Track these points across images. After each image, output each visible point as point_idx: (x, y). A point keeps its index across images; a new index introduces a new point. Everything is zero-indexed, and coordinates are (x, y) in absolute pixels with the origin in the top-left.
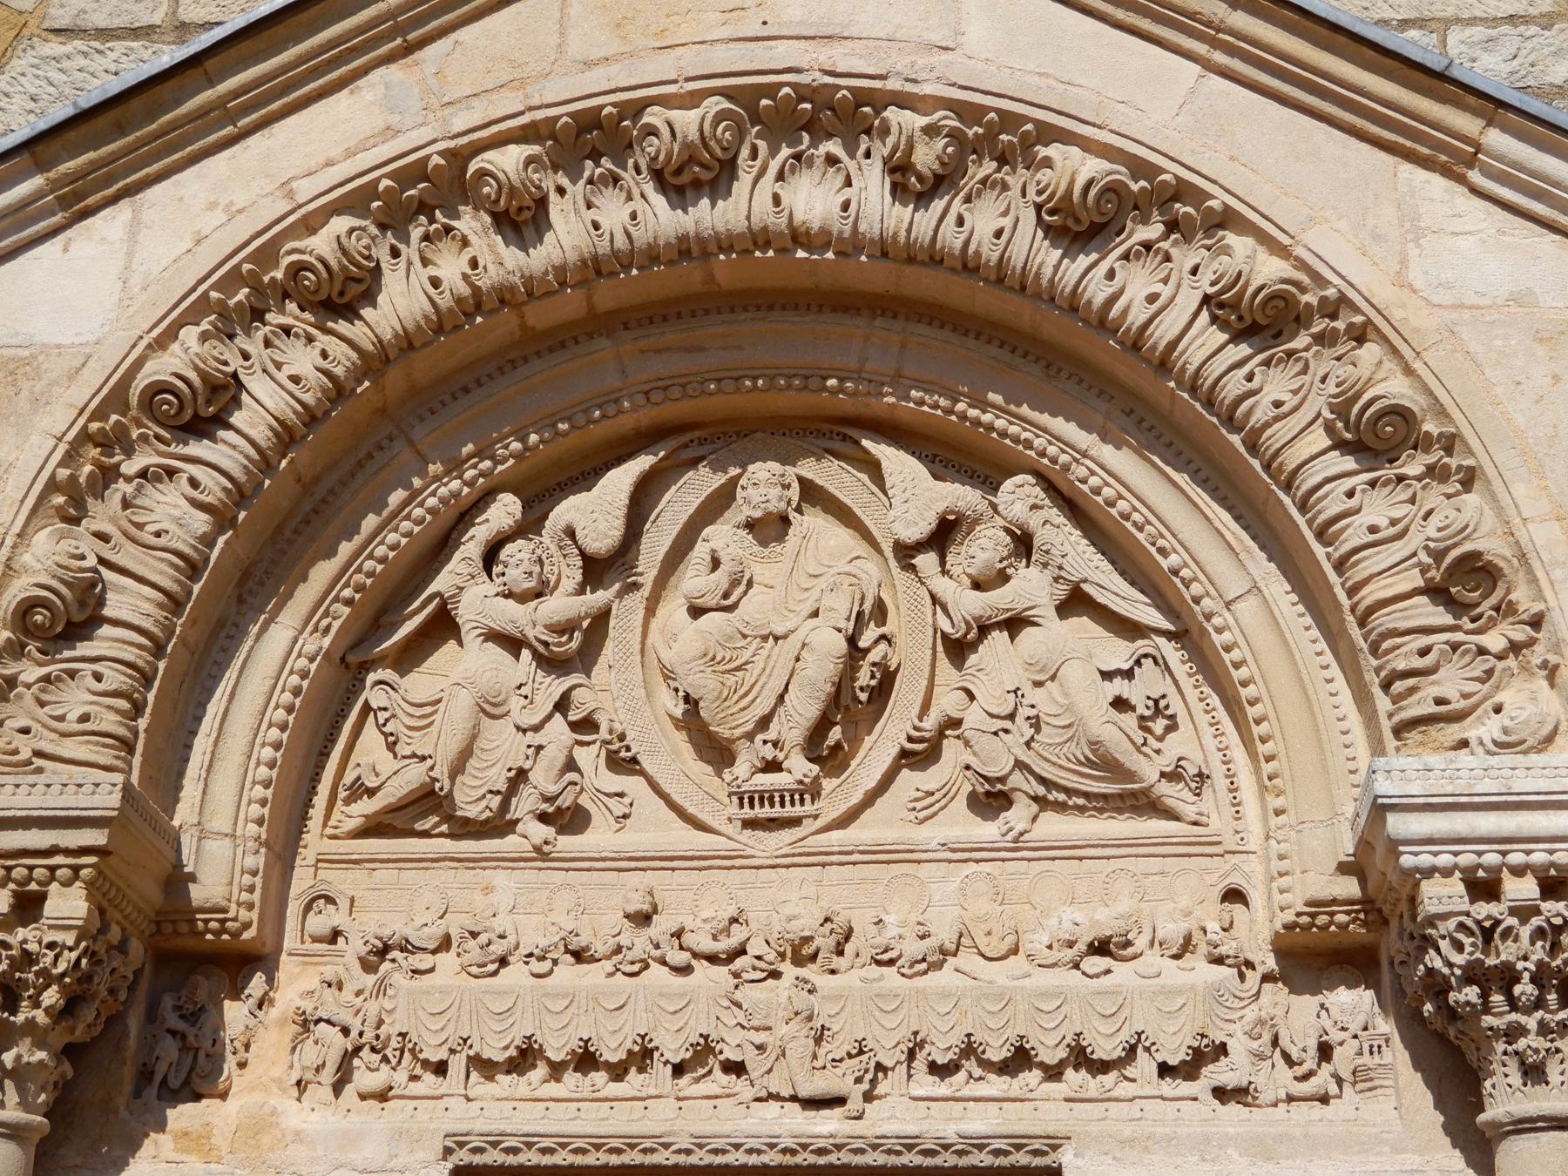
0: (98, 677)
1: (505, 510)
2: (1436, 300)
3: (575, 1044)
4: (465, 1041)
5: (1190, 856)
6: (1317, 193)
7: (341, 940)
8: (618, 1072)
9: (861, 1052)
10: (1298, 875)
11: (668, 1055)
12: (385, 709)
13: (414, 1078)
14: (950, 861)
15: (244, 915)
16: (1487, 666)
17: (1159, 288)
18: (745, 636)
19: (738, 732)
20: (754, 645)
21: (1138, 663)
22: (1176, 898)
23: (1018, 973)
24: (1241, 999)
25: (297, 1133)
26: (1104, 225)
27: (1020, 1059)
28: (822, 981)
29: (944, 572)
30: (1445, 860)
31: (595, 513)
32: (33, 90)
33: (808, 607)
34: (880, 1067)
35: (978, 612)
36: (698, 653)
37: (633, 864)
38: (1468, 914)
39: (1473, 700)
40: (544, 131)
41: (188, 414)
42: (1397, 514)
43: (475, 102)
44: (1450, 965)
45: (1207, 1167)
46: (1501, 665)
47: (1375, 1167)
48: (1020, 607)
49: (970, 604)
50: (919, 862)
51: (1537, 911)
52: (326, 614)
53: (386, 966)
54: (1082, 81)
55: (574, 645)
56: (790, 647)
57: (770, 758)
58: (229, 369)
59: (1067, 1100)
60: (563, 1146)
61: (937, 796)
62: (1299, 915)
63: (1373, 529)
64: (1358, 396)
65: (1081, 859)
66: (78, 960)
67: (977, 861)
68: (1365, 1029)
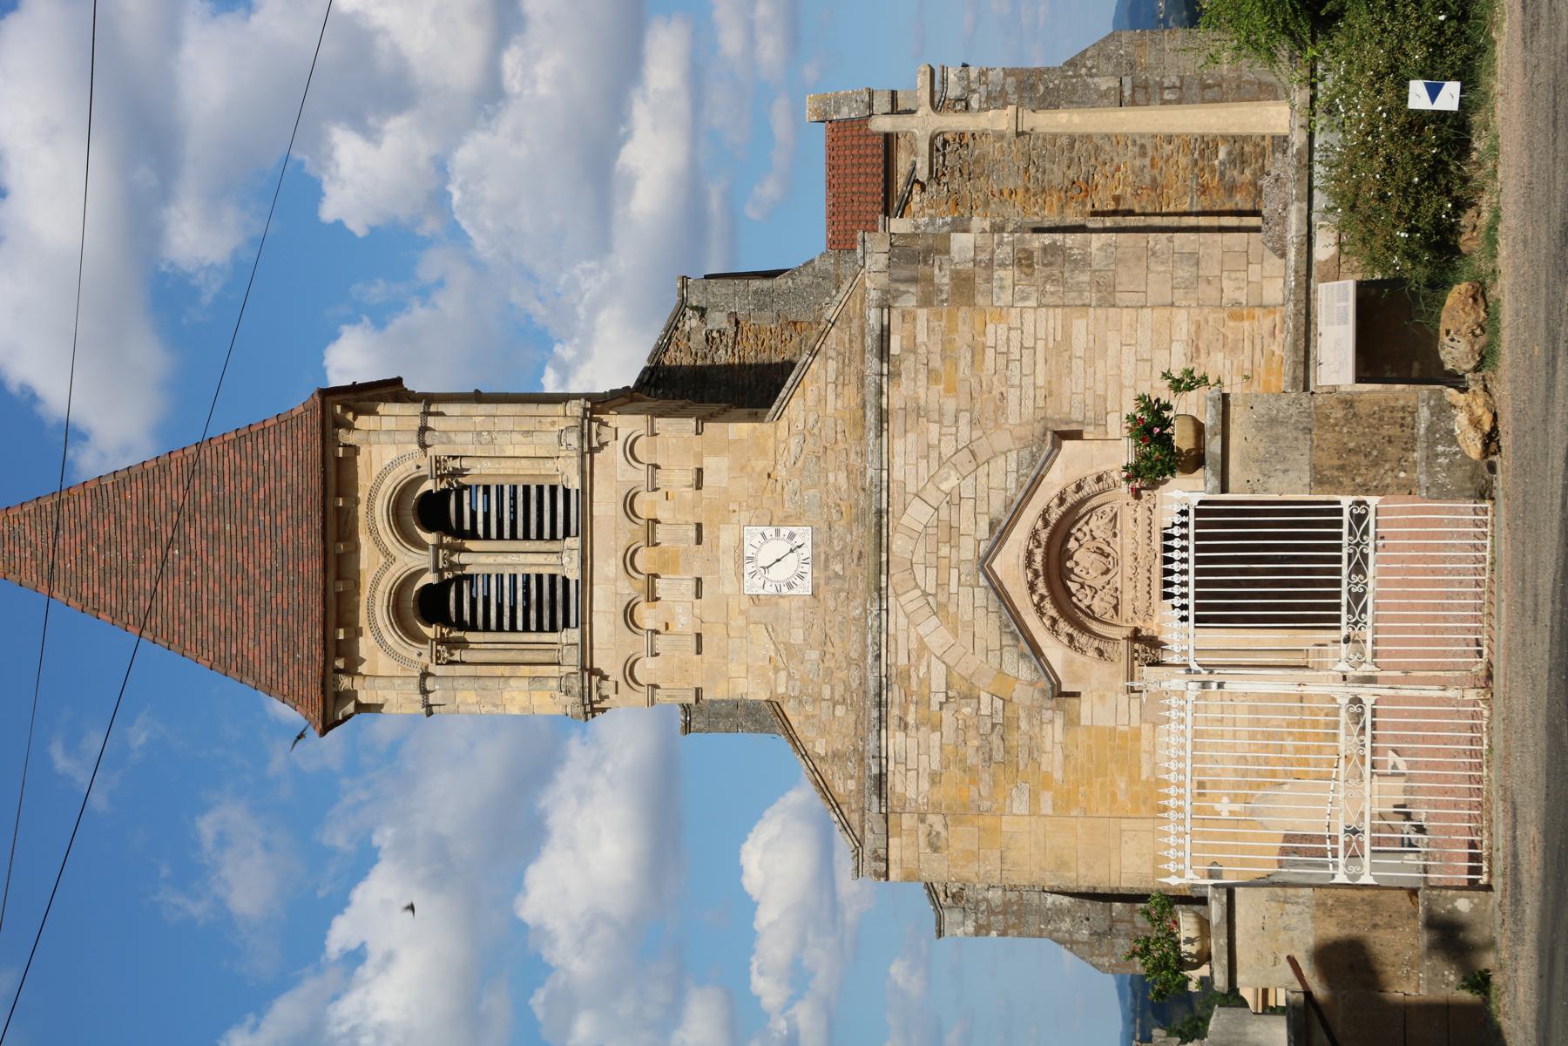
6: (1046, 494)
22: (1128, 511)
31: (1073, 587)
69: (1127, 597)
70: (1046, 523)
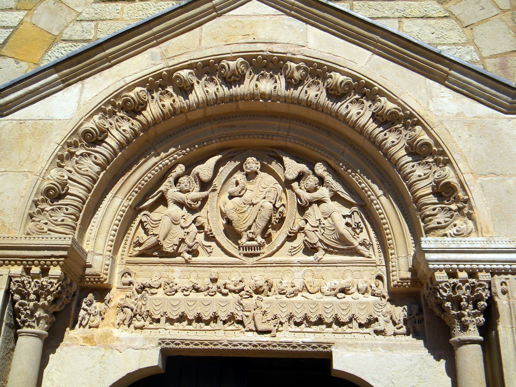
0: (67, 210)
1: (180, 169)
2: (437, 114)
3: (196, 314)
4: (165, 313)
5: (367, 266)
7: (132, 285)
8: (207, 323)
9: (275, 318)
10: (398, 272)
11: (222, 318)
12: (146, 222)
13: (151, 323)
14: (301, 266)
15: (105, 276)
16: (451, 214)
17: (360, 111)
18: (245, 204)
19: (243, 230)
20: (247, 207)
21: (353, 213)
22: (365, 277)
23: (319, 297)
24: (382, 306)
25: (117, 338)
26: (345, 94)
27: (320, 321)
28: (265, 298)
29: (300, 188)
30: (442, 266)
31: (205, 170)
32: (57, 55)
33: (263, 196)
34: (281, 323)
35: (309, 198)
36: (232, 208)
37: (213, 265)
38: (447, 282)
39: (448, 223)
40: (194, 66)
41: (94, 139)
42: (426, 172)
43: (175, 58)
44: (443, 296)
45: (372, 352)
46: (455, 213)
47: (420, 354)
48: (321, 197)
49: (306, 196)
50: (292, 266)
51: (467, 282)
52: (131, 195)
53: (144, 292)
54: (340, 55)
55: (198, 205)
56: (257, 207)
57: (251, 237)
58: (106, 127)
59: (333, 333)
60: (192, 343)
61: (297, 248)
62: (398, 282)
63: (420, 176)
64: (416, 139)
65: (337, 266)
66: (58, 287)
67: (308, 266)
68: (417, 315)
69: (179, 275)
70: (336, 94)
